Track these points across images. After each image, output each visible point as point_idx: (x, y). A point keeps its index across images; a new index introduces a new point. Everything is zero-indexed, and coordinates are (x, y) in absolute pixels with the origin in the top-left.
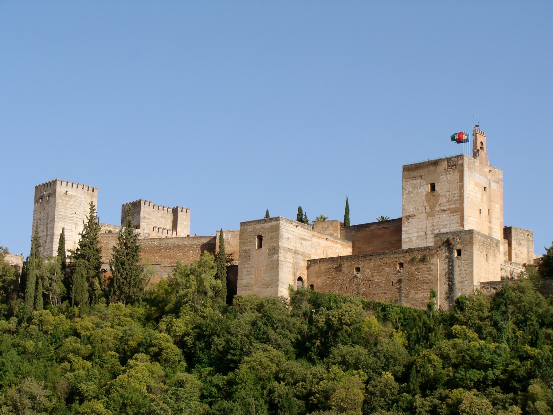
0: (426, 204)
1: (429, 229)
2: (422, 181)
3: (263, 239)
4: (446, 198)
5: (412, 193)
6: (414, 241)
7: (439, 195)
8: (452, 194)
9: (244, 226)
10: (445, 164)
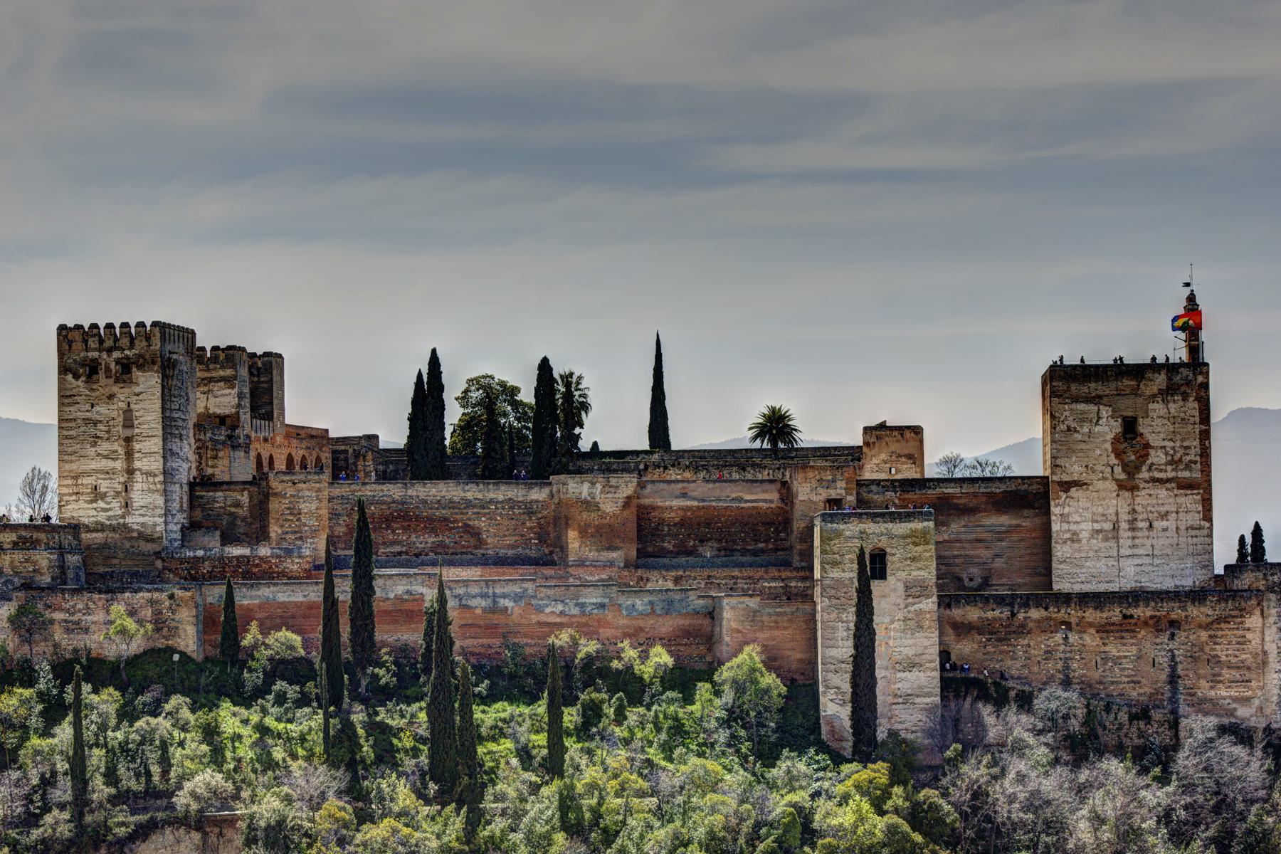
0: (1116, 462)
1: (1124, 517)
2: (1101, 407)
3: (889, 558)
4: (1166, 454)
5: (1076, 431)
6: (1084, 541)
7: (1147, 446)
8: (1181, 447)
9: (831, 522)
10: (1161, 380)
